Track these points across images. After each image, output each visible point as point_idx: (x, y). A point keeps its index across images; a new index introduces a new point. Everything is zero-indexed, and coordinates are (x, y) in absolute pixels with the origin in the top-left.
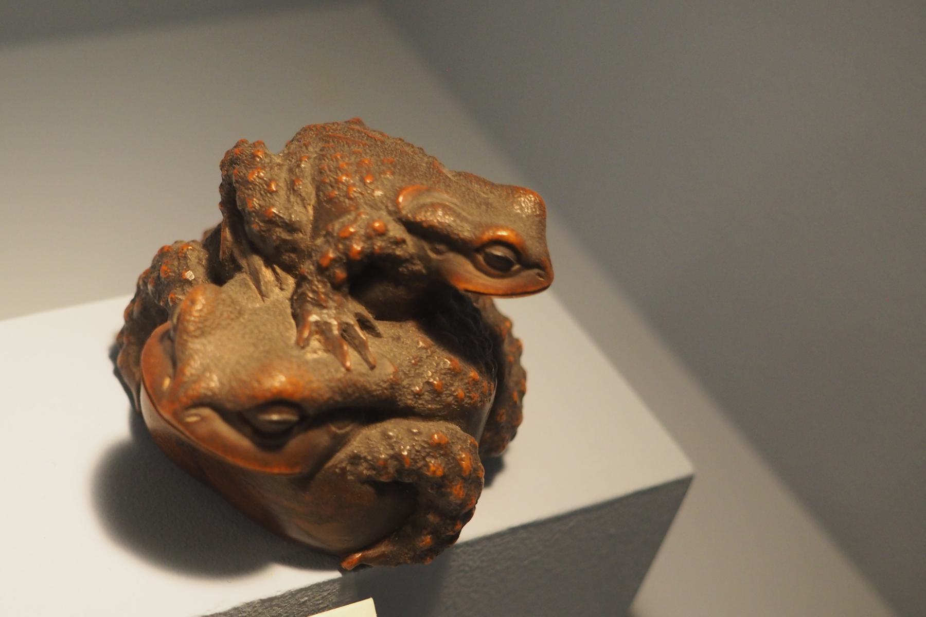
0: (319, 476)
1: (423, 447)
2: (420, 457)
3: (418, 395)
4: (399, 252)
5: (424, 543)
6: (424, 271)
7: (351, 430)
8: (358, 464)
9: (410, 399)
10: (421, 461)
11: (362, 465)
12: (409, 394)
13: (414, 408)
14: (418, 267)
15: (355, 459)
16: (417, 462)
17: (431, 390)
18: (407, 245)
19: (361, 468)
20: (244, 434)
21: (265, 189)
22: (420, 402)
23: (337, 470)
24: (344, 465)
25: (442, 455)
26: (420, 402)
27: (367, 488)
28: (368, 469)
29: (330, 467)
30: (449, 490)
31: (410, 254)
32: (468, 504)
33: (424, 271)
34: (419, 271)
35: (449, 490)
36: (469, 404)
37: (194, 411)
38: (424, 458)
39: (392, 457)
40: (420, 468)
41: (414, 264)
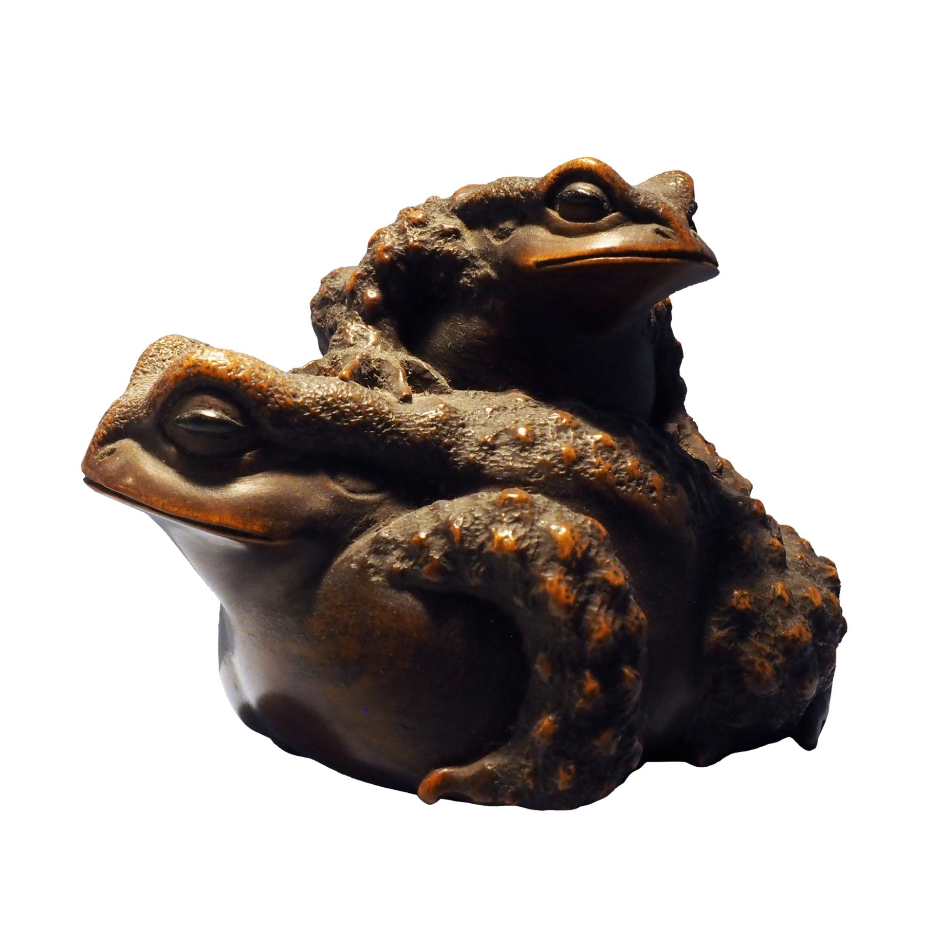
0: (328, 580)
1: (487, 512)
2: (480, 527)
3: (492, 447)
4: (449, 247)
5: (541, 730)
6: (493, 274)
7: (379, 504)
8: (386, 553)
9: (472, 452)
10: (483, 534)
11: (393, 555)
12: (471, 445)
13: (483, 467)
14: (485, 269)
15: (380, 547)
16: (477, 536)
17: (512, 440)
18: (464, 240)
19: (390, 559)
20: (170, 463)
21: (481, 459)
22: (492, 458)
23: (353, 566)
24: (363, 554)
25: (517, 520)
26: (492, 458)
27: (408, 600)
28: (402, 560)
29: (343, 561)
30: (541, 589)
31: (468, 252)
32: (592, 630)
33: (493, 274)
34: (487, 276)
35: (541, 589)
36: (593, 475)
37: (109, 447)
38: (486, 527)
39: (435, 532)
40: (482, 546)
41: (477, 267)
